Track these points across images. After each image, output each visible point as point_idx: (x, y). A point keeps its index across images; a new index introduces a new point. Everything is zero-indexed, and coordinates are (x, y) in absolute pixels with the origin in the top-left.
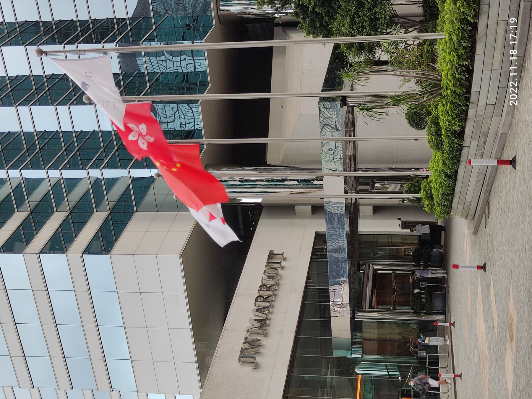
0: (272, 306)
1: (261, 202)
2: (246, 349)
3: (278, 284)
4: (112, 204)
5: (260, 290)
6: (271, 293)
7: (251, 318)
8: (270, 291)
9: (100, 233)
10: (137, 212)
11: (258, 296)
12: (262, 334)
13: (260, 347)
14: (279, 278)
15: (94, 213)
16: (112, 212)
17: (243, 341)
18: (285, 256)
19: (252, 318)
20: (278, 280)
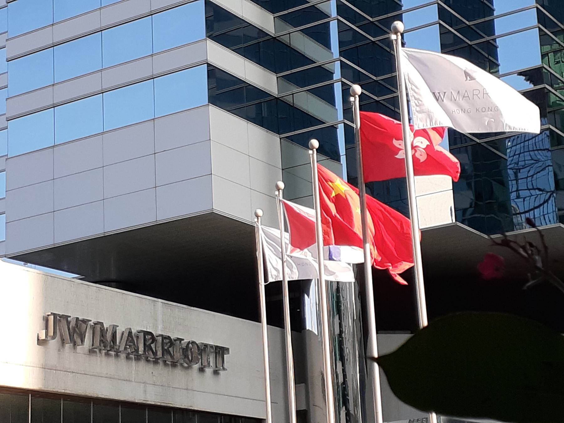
0: (138, 358)
1: (307, 328)
2: (68, 323)
3: (174, 365)
4: (289, 99)
5: (164, 337)
6: (159, 354)
7: (118, 326)
8: (163, 354)
9: (243, 85)
10: (281, 139)
11: (154, 334)
12: (93, 345)
13: (72, 344)
14: (186, 365)
15: (275, 73)
16: (278, 101)
17: (80, 318)
18: (221, 372)
19: (117, 328)
20: (181, 365)
